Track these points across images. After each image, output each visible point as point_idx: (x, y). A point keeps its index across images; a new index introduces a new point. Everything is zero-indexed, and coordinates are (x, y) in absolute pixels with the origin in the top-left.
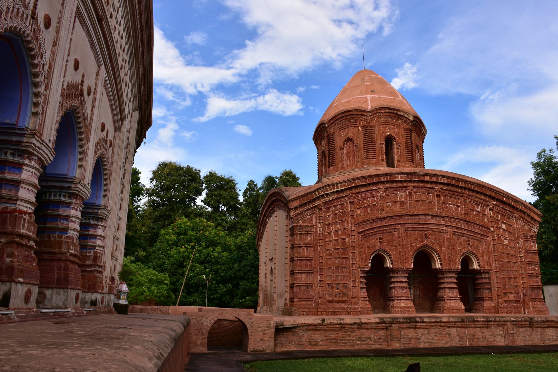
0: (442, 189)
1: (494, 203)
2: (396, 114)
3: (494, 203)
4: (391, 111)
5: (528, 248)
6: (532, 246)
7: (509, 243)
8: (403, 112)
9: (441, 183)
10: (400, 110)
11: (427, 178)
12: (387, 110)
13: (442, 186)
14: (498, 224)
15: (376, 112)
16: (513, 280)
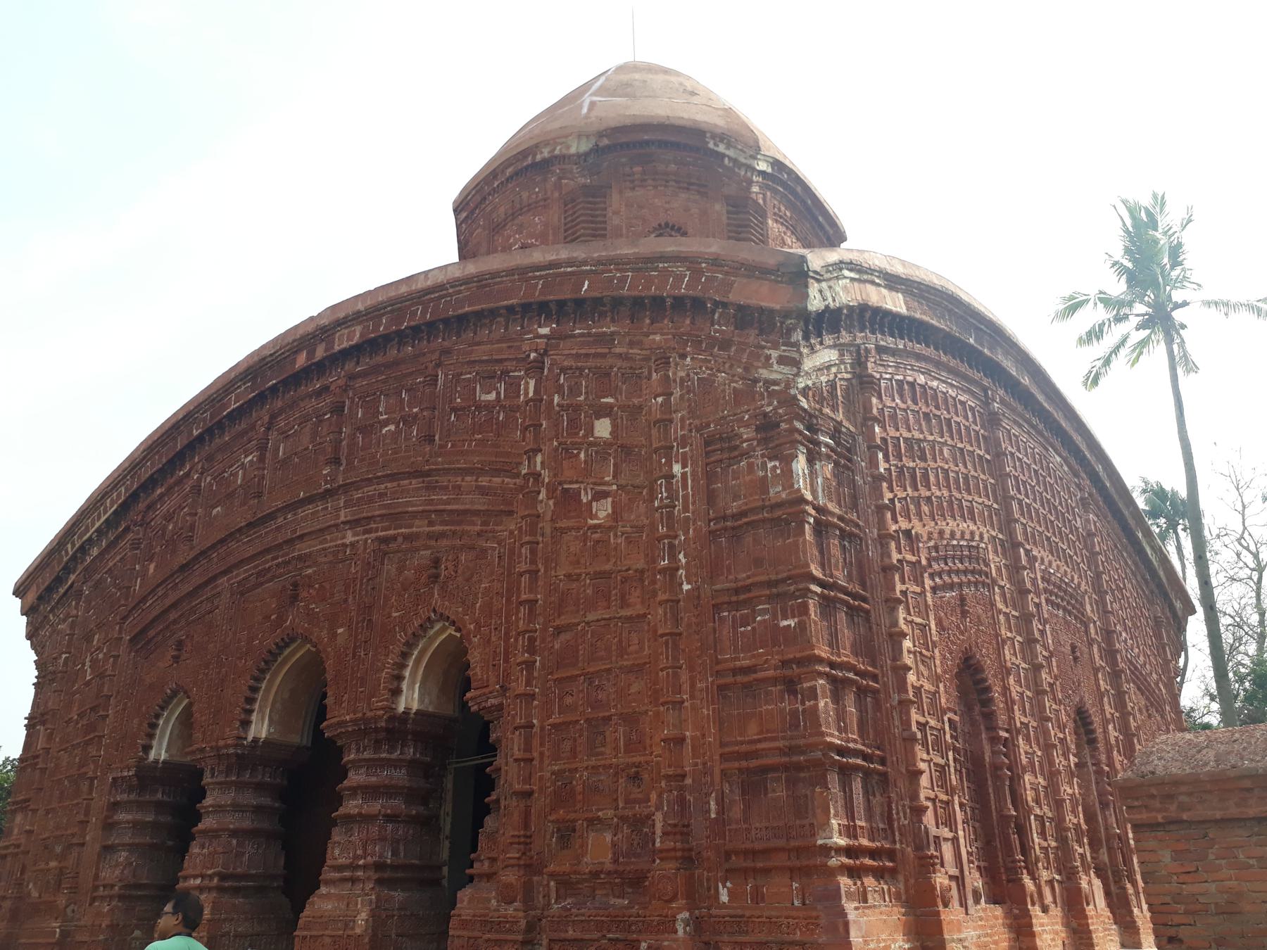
0: (352, 377)
1: (544, 331)
2: (534, 165)
3: (544, 331)
4: (520, 166)
5: (735, 507)
6: (763, 485)
7: (616, 515)
8: (547, 143)
9: (346, 354)
10: (537, 146)
11: (301, 360)
12: (509, 171)
13: (349, 366)
14: (574, 424)
15: (478, 198)
16: (620, 733)
